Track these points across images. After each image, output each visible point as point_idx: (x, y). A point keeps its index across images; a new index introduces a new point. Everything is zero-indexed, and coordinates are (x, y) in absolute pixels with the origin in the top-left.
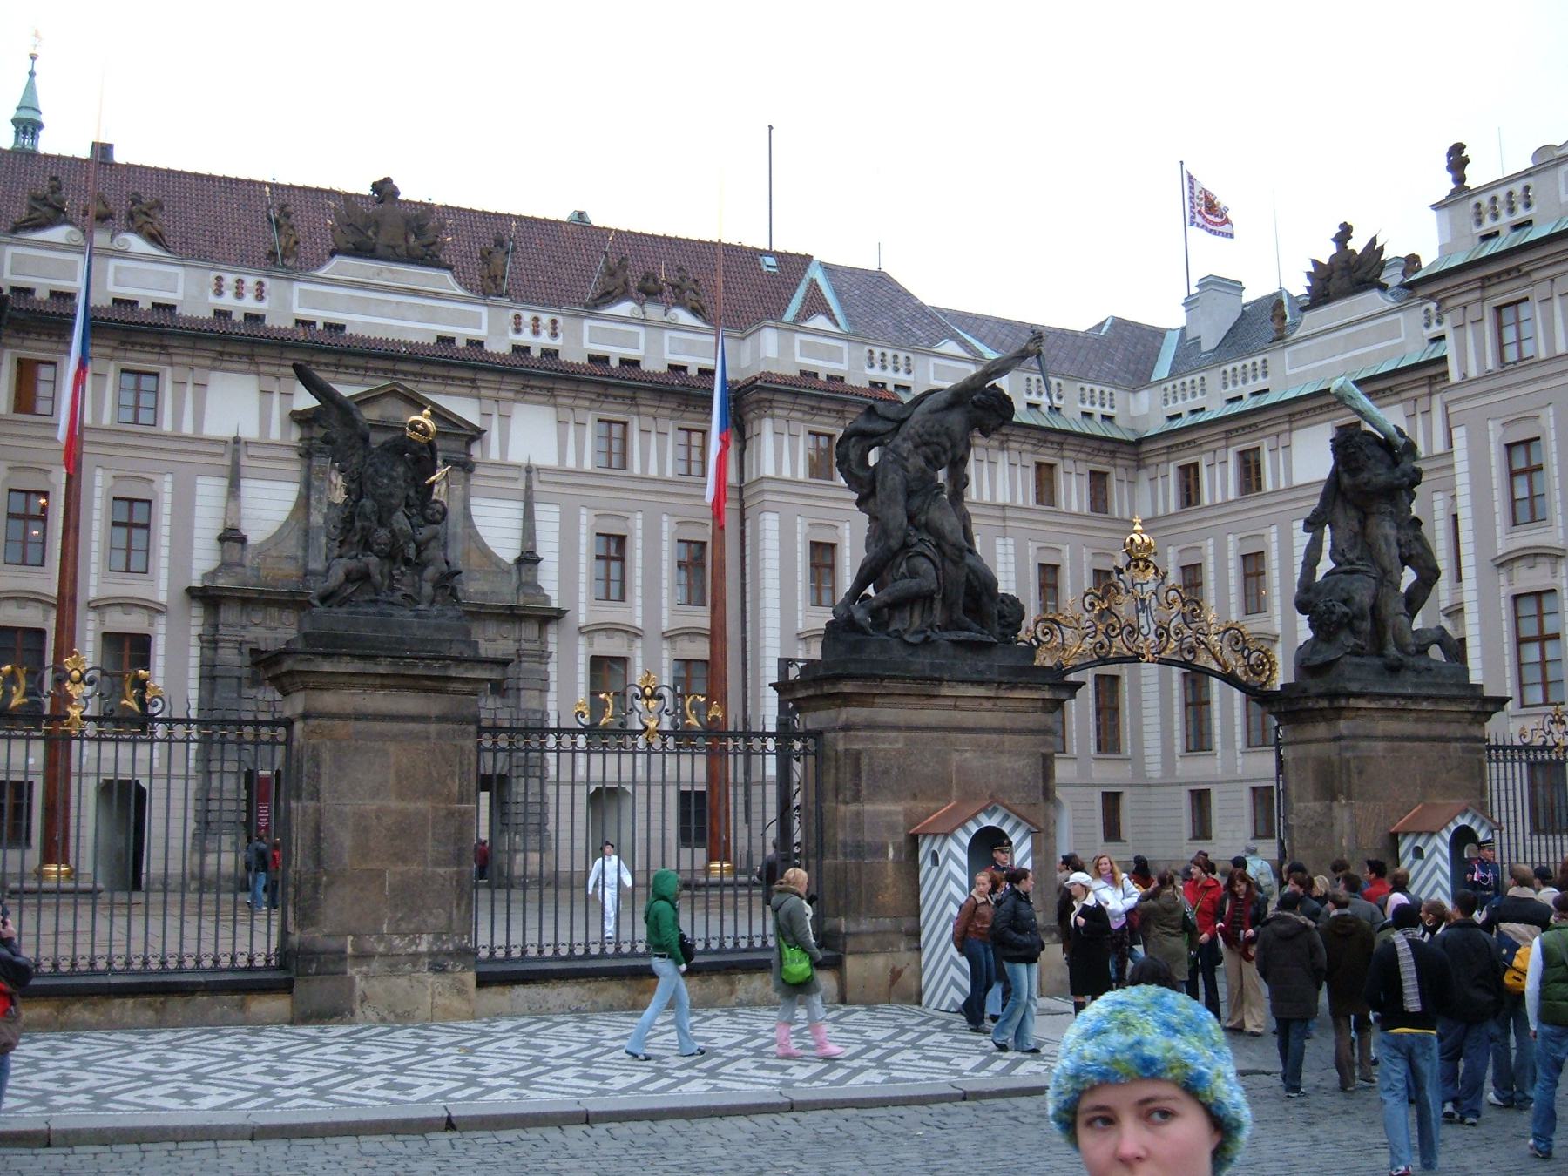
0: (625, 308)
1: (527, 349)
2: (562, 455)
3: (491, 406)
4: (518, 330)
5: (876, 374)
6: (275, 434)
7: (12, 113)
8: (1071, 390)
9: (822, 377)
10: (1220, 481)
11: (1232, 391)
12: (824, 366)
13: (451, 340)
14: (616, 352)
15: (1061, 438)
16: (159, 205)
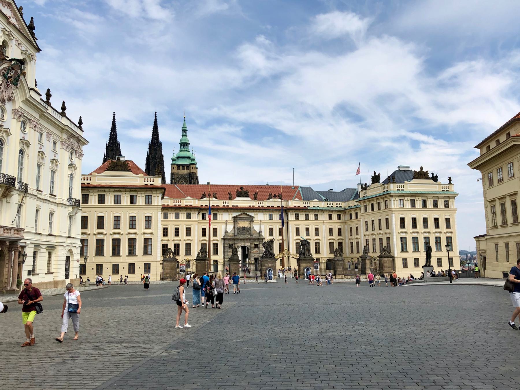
0: (272, 200)
1: (260, 206)
2: (264, 219)
3: (255, 214)
4: (258, 204)
5: (305, 205)
6: (231, 220)
7: (182, 129)
8: (334, 203)
9: (297, 206)
10: (354, 217)
11: (355, 204)
12: (297, 205)
13: (250, 206)
14: (271, 205)
15: (333, 211)
16: (216, 194)
